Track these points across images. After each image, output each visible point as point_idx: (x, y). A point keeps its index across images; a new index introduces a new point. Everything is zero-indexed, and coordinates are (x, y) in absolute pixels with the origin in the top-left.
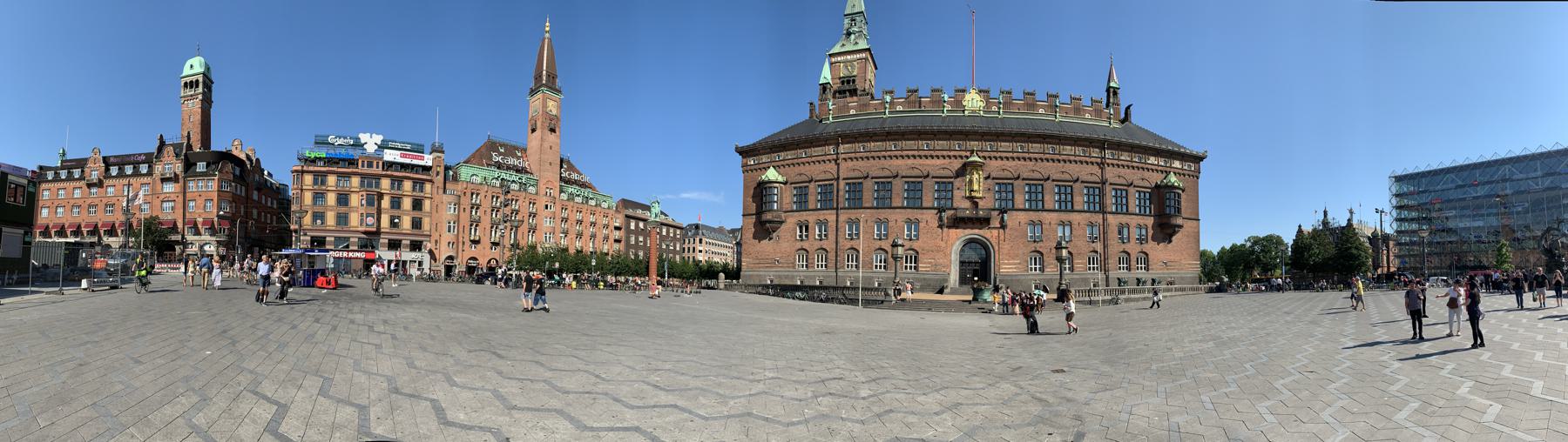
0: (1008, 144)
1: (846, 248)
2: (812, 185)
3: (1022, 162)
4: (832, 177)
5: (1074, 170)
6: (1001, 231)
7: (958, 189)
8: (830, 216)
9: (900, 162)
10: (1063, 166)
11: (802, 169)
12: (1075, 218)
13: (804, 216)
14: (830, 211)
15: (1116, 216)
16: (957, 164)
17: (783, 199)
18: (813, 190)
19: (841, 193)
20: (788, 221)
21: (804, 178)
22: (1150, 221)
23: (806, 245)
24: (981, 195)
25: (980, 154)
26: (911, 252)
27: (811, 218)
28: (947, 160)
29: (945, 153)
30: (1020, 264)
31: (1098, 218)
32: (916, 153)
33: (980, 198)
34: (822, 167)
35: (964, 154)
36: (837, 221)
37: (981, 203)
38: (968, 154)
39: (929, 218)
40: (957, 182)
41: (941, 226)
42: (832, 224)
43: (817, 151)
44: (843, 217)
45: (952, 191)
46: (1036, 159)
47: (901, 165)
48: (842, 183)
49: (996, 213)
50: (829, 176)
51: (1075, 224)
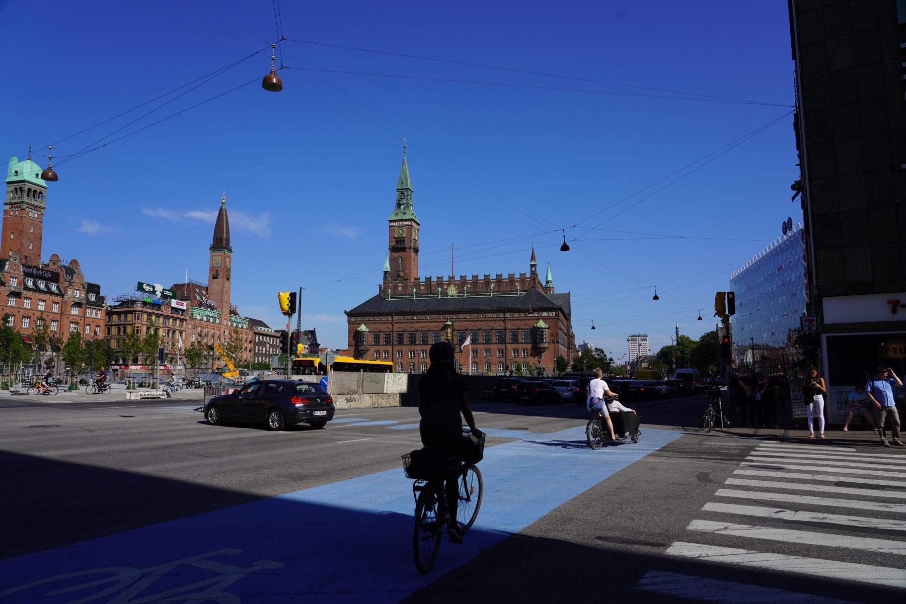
2: (381, 334)
4: (390, 330)
5: (492, 325)
6: (460, 353)
8: (389, 348)
9: (418, 324)
11: (377, 326)
12: (493, 347)
13: (378, 348)
15: (511, 345)
16: (442, 325)
17: (369, 340)
18: (382, 336)
19: (394, 338)
20: (371, 349)
21: (378, 330)
22: (529, 346)
25: (451, 320)
27: (381, 348)
28: (438, 323)
29: (437, 320)
31: (503, 346)
32: (424, 321)
34: (386, 325)
35: (444, 320)
36: (393, 351)
38: (446, 320)
40: (442, 333)
42: (390, 352)
43: (384, 318)
44: (396, 349)
45: (440, 336)
46: (475, 321)
47: (420, 326)
48: (395, 333)
49: (458, 346)
50: (389, 330)
51: (492, 350)
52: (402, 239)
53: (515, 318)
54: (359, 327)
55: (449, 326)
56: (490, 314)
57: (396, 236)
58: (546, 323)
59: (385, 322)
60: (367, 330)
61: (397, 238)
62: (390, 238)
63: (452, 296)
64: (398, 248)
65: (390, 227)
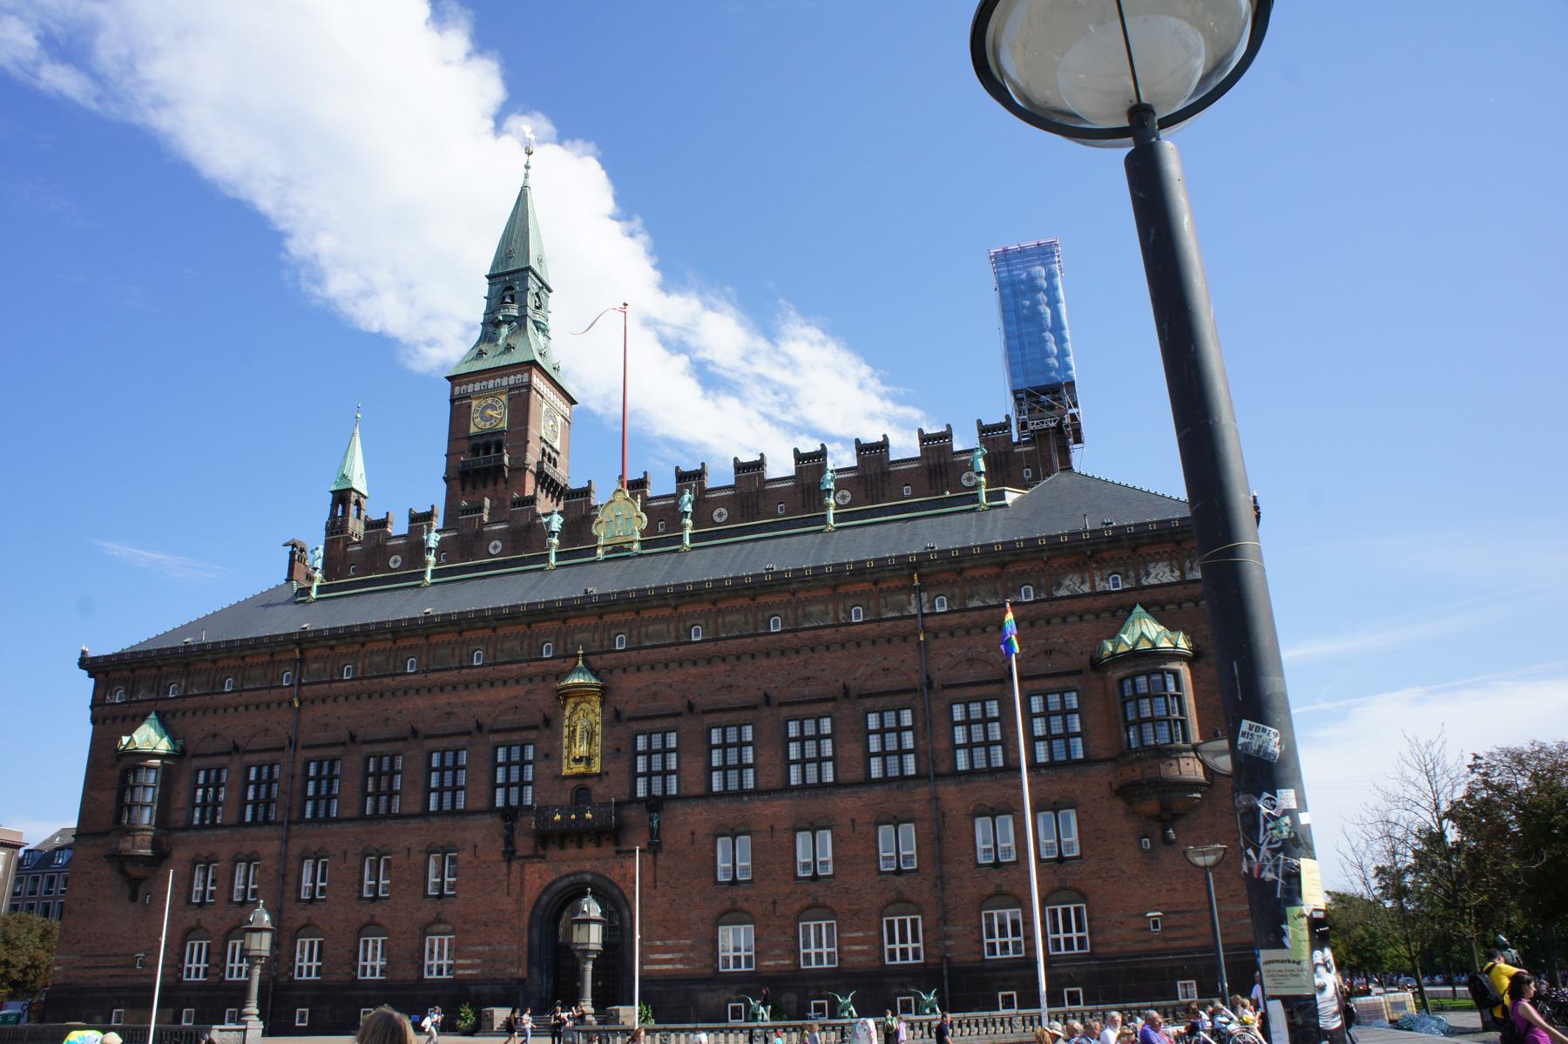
0: (662, 627)
1: (296, 925)
2: (236, 762)
3: (703, 669)
7: (547, 756)
9: (421, 702)
10: (806, 663)
14: (267, 830)
23: (207, 917)
24: (596, 768)
26: (442, 926)
30: (692, 948)
32: (451, 676)
33: (599, 775)
37: (598, 789)
38: (571, 661)
39: (484, 834)
41: (510, 855)
52: (495, 438)
53: (975, 615)
54: (130, 733)
55: (580, 692)
56: (816, 608)
57: (473, 430)
58: (1171, 625)
59: (265, 696)
60: (163, 746)
61: (476, 436)
62: (452, 439)
63: (618, 548)
64: (476, 472)
65: (452, 401)
